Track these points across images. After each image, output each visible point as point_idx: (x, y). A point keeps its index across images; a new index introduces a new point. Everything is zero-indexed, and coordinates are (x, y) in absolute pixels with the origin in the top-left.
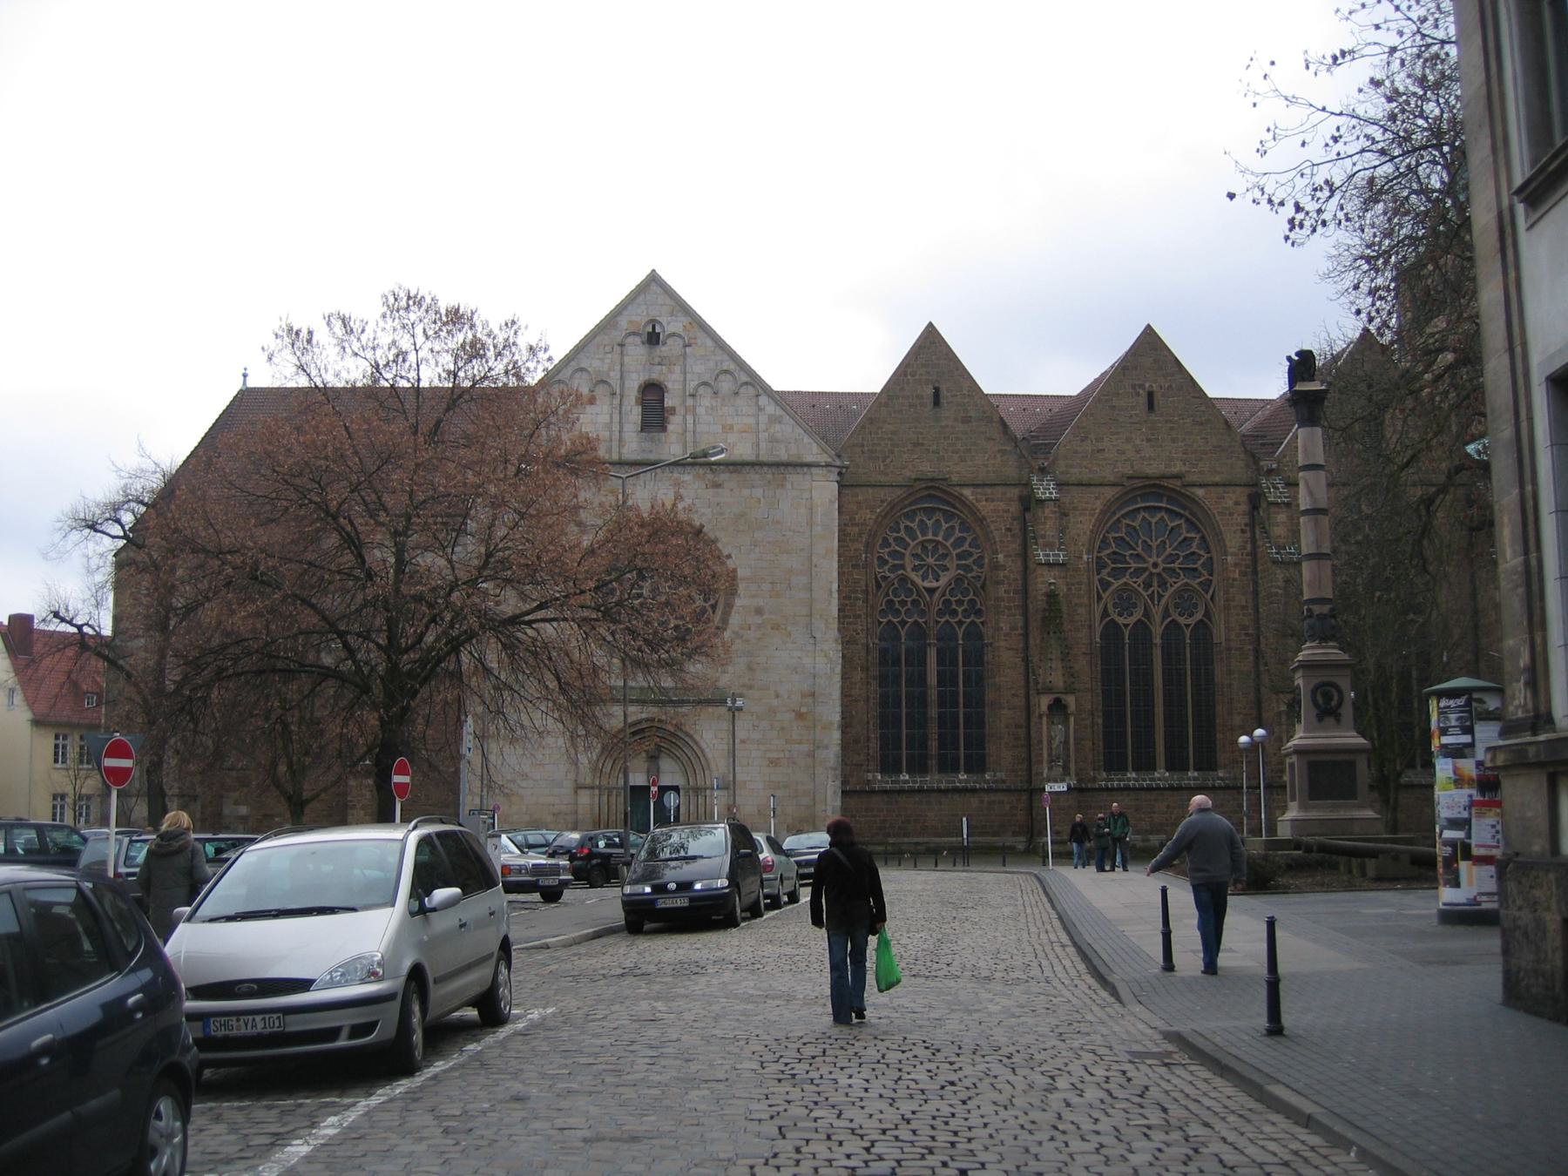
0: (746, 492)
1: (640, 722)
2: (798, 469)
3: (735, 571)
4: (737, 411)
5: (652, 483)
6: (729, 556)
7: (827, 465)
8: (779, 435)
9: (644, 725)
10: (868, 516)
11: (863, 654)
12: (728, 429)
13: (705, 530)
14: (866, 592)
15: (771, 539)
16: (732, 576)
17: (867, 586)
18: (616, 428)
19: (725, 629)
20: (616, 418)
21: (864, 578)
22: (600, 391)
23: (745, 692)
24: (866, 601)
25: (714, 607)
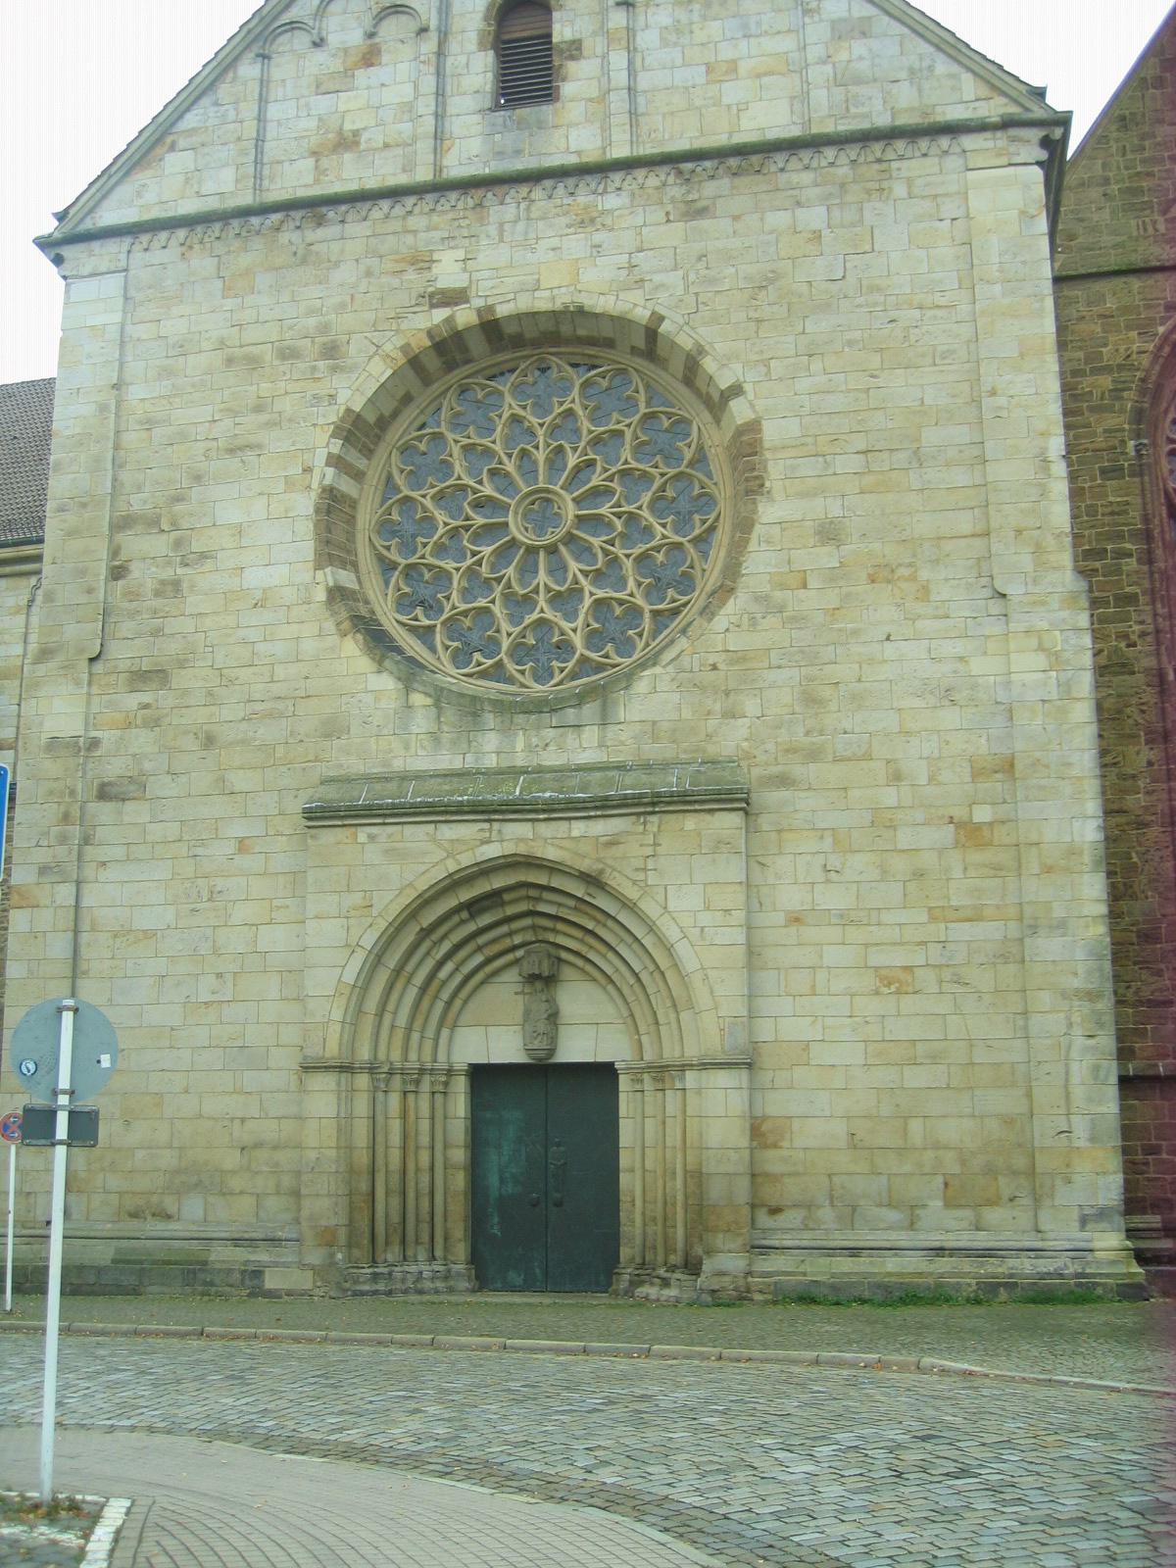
0: (779, 219)
1: (486, 870)
2: (924, 144)
3: (753, 427)
4: (745, 26)
5: (521, 226)
6: (736, 390)
7: (1007, 124)
8: (863, 67)
9: (498, 882)
10: (1135, 347)
11: (1150, 696)
12: (720, 71)
13: (665, 328)
14: (1148, 536)
15: (857, 335)
16: (747, 447)
17: (1146, 519)
18: (426, 107)
19: (732, 590)
20: (429, 83)
21: (1139, 500)
22: (391, 28)
23: (798, 770)
24: (1148, 558)
25: (702, 541)
